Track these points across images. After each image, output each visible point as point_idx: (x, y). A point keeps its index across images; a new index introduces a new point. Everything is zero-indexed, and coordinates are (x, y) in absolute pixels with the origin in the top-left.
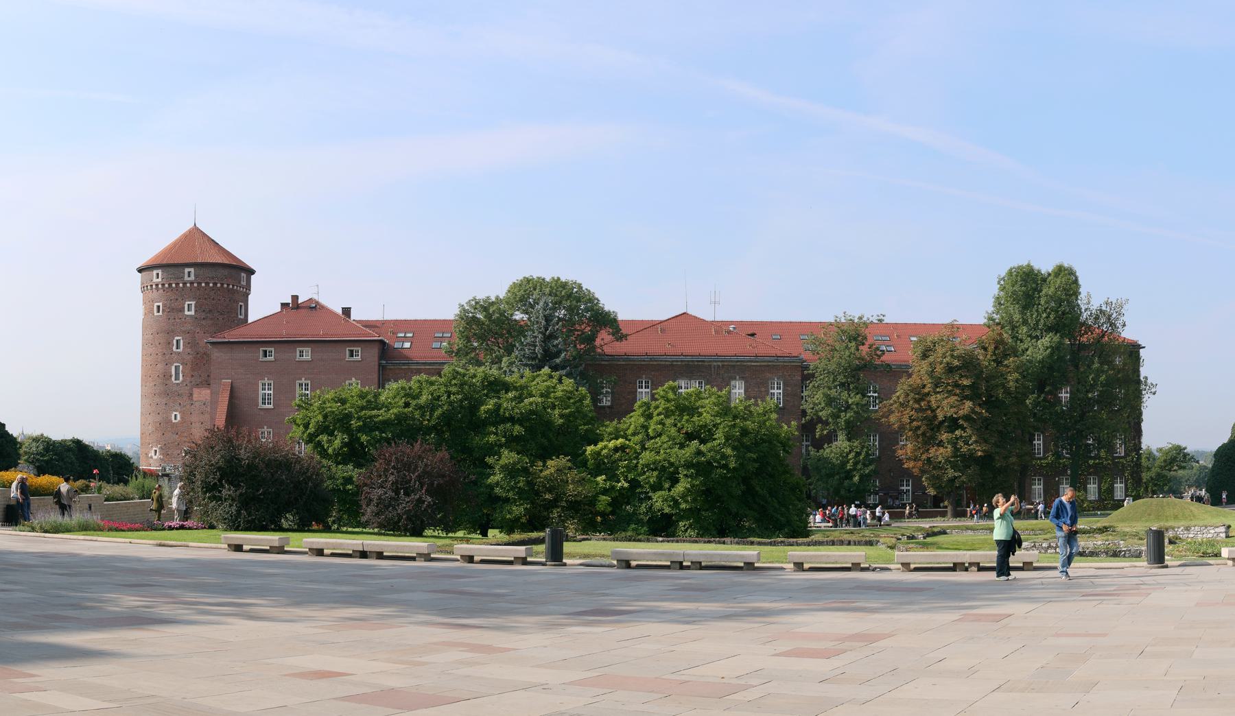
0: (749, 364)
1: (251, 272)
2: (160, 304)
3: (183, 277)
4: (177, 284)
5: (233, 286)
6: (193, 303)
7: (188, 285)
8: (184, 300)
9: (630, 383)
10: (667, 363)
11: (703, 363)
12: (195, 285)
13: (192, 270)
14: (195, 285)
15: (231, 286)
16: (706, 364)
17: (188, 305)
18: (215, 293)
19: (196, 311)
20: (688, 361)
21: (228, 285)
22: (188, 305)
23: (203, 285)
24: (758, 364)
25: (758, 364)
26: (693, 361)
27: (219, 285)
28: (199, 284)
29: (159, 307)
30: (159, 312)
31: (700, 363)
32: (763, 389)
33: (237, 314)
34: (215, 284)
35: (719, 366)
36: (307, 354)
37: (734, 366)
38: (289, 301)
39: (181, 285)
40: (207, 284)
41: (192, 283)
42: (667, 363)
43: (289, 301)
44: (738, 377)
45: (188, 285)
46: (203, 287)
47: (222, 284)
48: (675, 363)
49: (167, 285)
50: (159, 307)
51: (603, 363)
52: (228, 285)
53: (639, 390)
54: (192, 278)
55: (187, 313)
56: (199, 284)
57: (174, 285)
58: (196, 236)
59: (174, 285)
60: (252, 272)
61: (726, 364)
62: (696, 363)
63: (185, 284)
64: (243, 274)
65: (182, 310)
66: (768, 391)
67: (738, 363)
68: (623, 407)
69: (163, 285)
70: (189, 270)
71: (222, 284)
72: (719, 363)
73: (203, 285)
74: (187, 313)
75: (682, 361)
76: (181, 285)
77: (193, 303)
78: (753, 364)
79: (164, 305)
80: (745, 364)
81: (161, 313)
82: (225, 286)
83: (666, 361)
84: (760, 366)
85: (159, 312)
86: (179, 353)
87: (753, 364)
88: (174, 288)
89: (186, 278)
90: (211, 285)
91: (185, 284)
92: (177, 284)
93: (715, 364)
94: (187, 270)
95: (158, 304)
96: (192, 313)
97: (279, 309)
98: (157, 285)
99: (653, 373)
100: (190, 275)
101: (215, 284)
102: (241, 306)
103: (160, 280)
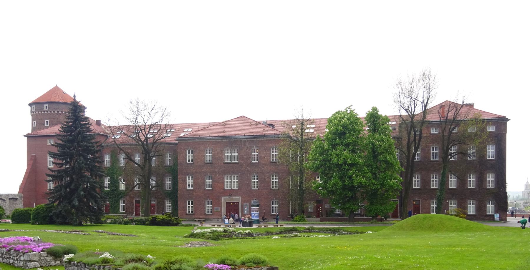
0: (261, 139)
2: (35, 121)
3: (44, 109)
4: (41, 112)
6: (48, 121)
7: (46, 112)
8: (45, 119)
9: (202, 151)
10: (220, 140)
11: (238, 140)
12: (49, 112)
13: (47, 105)
19: (49, 124)
23: (52, 112)
24: (265, 139)
25: (265, 139)
27: (60, 112)
28: (51, 111)
29: (35, 122)
31: (236, 140)
32: (268, 152)
34: (58, 112)
35: (245, 141)
37: (253, 141)
39: (43, 112)
40: (54, 111)
41: (47, 111)
42: (220, 140)
44: (255, 147)
45: (46, 112)
46: (53, 113)
47: (62, 112)
48: (223, 140)
49: (37, 113)
56: (51, 111)
57: (40, 113)
59: (40, 113)
61: (249, 139)
62: (234, 140)
65: (44, 124)
66: (259, 154)
67: (255, 139)
68: (199, 163)
69: (36, 112)
71: (62, 112)
72: (246, 140)
73: (52, 112)
75: (227, 139)
76: (43, 112)
77: (48, 121)
78: (263, 139)
80: (259, 139)
81: (35, 126)
84: (266, 140)
87: (263, 139)
88: (40, 114)
89: (45, 109)
90: (56, 112)
91: (44, 112)
92: (41, 112)
93: (244, 140)
94: (45, 105)
98: (33, 112)
99: (213, 146)
100: (46, 107)
101: (58, 112)
103: (34, 110)
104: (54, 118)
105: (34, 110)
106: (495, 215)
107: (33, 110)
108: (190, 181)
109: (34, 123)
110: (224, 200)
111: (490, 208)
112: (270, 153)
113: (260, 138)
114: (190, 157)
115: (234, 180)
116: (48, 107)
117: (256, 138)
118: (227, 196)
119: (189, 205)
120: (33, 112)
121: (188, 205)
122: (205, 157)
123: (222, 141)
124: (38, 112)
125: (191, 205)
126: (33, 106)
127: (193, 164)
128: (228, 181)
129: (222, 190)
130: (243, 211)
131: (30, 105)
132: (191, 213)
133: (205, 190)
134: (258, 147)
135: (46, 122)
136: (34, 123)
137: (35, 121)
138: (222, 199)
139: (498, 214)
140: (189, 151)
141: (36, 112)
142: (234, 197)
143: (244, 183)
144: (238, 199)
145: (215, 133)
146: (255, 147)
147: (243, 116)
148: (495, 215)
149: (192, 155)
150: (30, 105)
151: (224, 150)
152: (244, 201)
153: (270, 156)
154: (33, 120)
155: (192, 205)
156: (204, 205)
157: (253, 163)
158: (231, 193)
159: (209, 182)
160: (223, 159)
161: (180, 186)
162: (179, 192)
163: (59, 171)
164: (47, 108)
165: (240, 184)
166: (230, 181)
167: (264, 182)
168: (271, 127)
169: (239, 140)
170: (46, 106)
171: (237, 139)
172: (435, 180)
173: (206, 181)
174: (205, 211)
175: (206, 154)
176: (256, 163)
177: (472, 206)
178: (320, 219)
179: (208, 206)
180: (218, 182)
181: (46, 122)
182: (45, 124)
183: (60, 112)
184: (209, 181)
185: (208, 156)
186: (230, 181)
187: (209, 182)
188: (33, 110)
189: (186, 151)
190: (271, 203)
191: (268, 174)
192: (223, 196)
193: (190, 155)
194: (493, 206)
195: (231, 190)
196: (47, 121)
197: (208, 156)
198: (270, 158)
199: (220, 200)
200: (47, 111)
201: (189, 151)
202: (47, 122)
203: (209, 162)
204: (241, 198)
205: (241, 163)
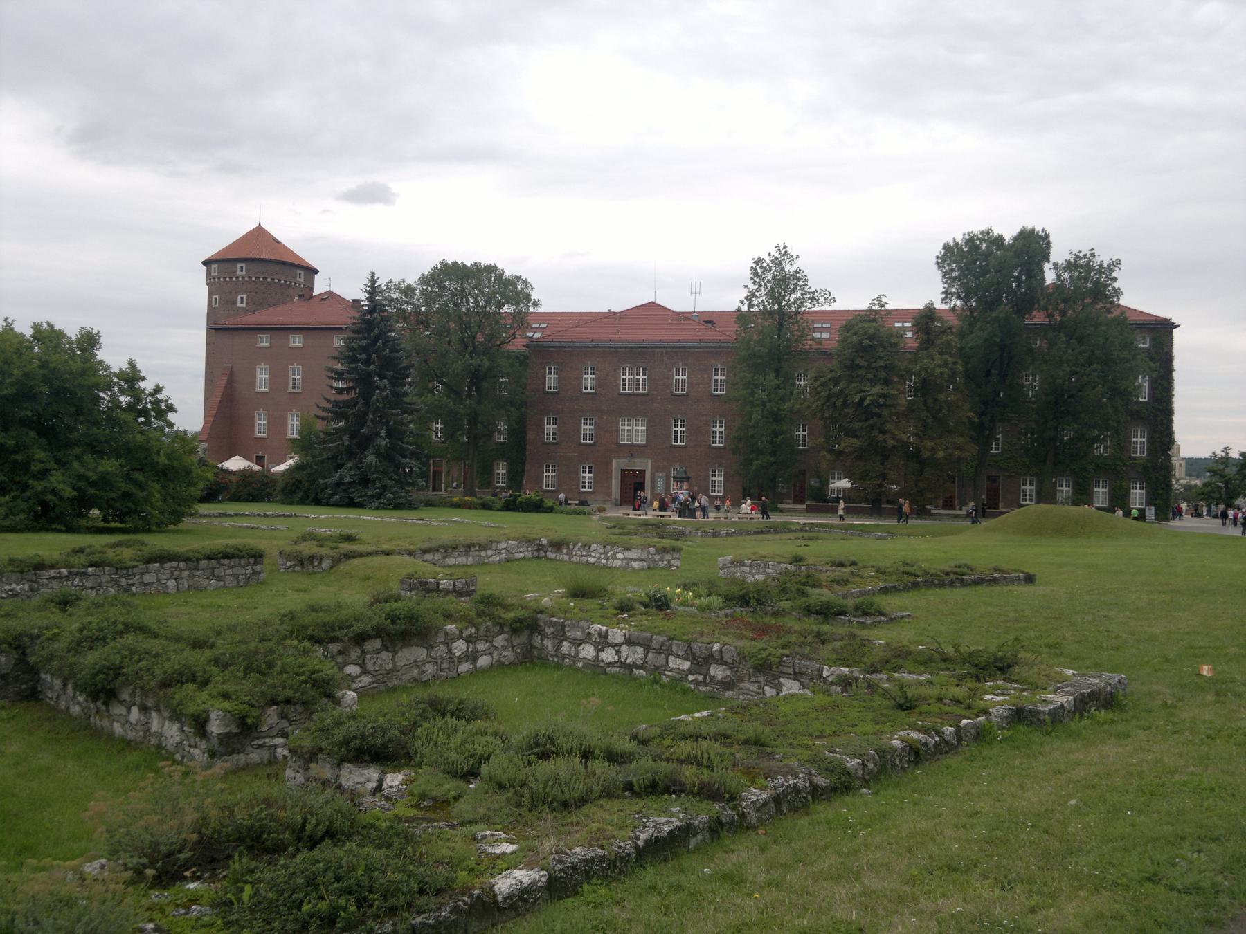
0: (692, 350)
1: (316, 272)
2: (217, 297)
3: (236, 272)
4: (231, 278)
5: (285, 281)
6: (245, 296)
7: (240, 279)
12: (246, 279)
13: (243, 265)
14: (246, 279)
15: (283, 282)
16: (650, 350)
18: (266, 287)
19: (247, 304)
20: (631, 348)
21: (279, 280)
23: (254, 279)
26: (636, 348)
27: (269, 280)
28: (250, 278)
29: (216, 299)
32: (706, 376)
35: (662, 352)
36: (296, 341)
39: (234, 279)
40: (257, 278)
41: (243, 277)
44: (680, 364)
45: (240, 279)
47: (273, 279)
50: (216, 299)
51: (551, 349)
52: (279, 280)
53: (585, 376)
54: (244, 273)
55: (239, 305)
56: (250, 278)
57: (228, 279)
58: (259, 232)
59: (228, 279)
60: (316, 272)
63: (237, 278)
64: (299, 271)
65: (235, 302)
69: (219, 278)
71: (273, 279)
72: (664, 350)
73: (254, 279)
74: (239, 305)
75: (626, 348)
76: (234, 279)
77: (245, 296)
79: (220, 298)
81: (217, 306)
82: (276, 281)
83: (610, 348)
89: (239, 273)
90: (261, 279)
91: (237, 278)
92: (231, 278)
94: (239, 265)
95: (215, 297)
98: (214, 279)
100: (241, 270)
101: (265, 279)
103: (216, 274)
104: (256, 290)
105: (216, 274)
106: (1147, 508)
107: (213, 274)
108: (550, 428)
109: (213, 300)
110: (617, 465)
111: (1138, 496)
112: (711, 378)
113: (691, 348)
114: (551, 379)
115: (637, 428)
117: (684, 347)
118: (624, 457)
119: (547, 474)
120: (214, 279)
121: (545, 474)
122: (581, 381)
123: (617, 352)
124: (225, 278)
125: (551, 474)
126: (213, 266)
127: (557, 393)
128: (626, 428)
129: (613, 446)
130: (653, 488)
131: (206, 263)
132: (550, 488)
133: (581, 444)
134: (686, 364)
135: (239, 299)
136: (213, 300)
137: (217, 297)
138: (614, 462)
139: (1153, 508)
140: (550, 368)
141: (219, 278)
142: (637, 461)
143: (657, 432)
144: (644, 464)
145: (602, 334)
146: (680, 364)
147: (652, 302)
148: (1147, 508)
149: (556, 376)
150: (206, 263)
151: (619, 369)
152: (656, 469)
153: (709, 383)
154: (210, 294)
155: (554, 474)
156: (578, 474)
157: (676, 395)
158: (633, 451)
159: (588, 428)
160: (618, 385)
161: (530, 435)
162: (528, 447)
163: (336, 402)
164: (242, 271)
165: (650, 434)
166: (630, 428)
167: (697, 431)
168: (710, 325)
169: (650, 350)
170: (242, 268)
171: (646, 348)
172: (1139, 440)
173: (583, 427)
174: (578, 485)
175: (585, 376)
176: (683, 395)
177: (1101, 490)
178: (804, 506)
179: (584, 475)
180: (607, 430)
181: (239, 299)
182: (236, 303)
183: (269, 280)
184: (588, 427)
185: (589, 379)
186: (630, 428)
187: (588, 428)
188: (213, 274)
189: (544, 368)
190: (709, 473)
191: (705, 418)
192: (615, 457)
193: (553, 376)
194: (1144, 491)
195: (632, 445)
197: (589, 379)
198: (710, 387)
199: (609, 464)
200: (243, 277)
201: (550, 368)
202: (242, 298)
203: (589, 390)
204: (650, 462)
205: (653, 394)
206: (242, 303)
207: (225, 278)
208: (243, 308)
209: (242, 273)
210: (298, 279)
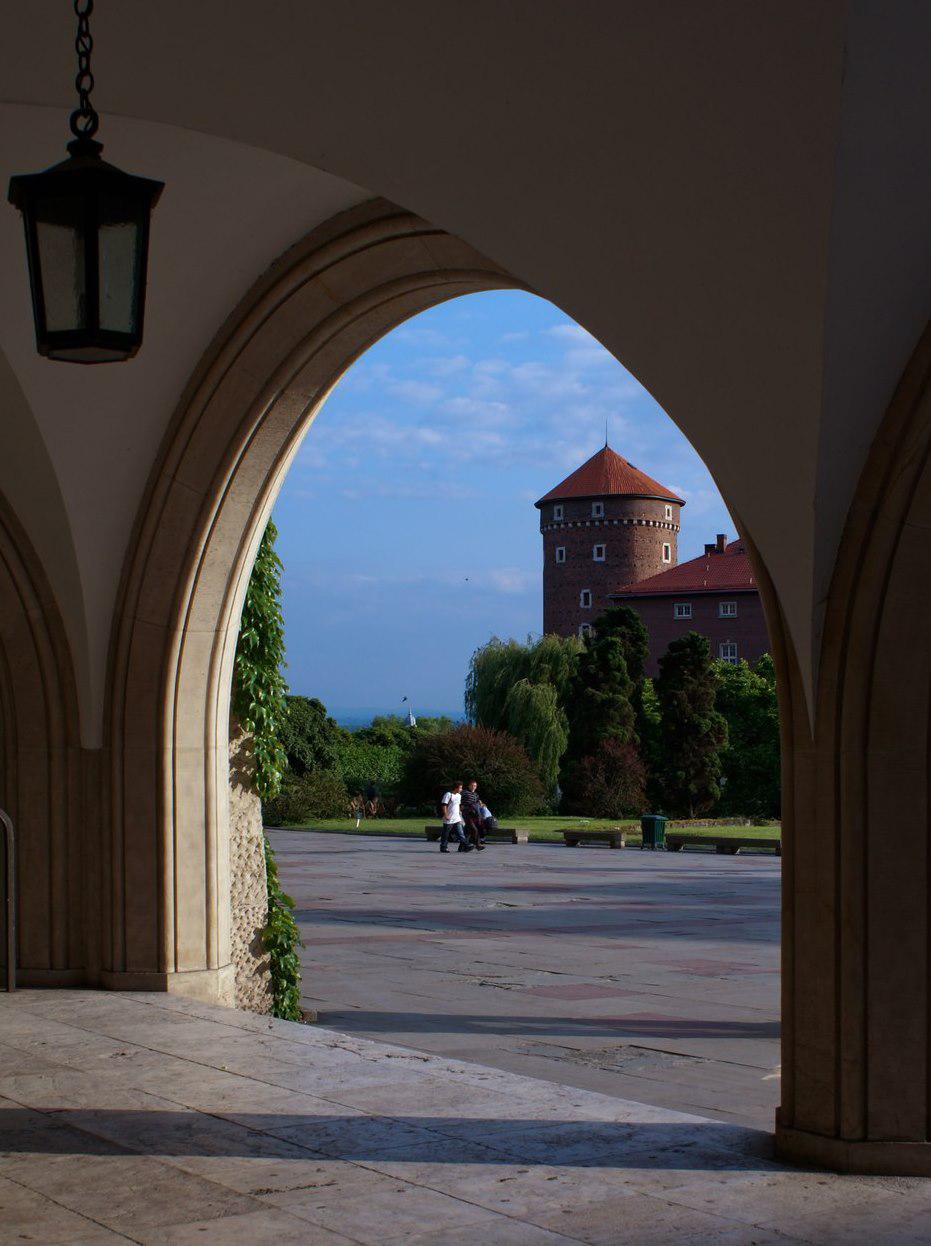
2: (563, 548)
4: (583, 523)
6: (603, 546)
7: (597, 523)
8: (592, 543)
12: (606, 523)
13: (601, 504)
14: (606, 523)
17: (598, 549)
19: (607, 556)
22: (598, 549)
23: (615, 522)
29: (561, 552)
30: (561, 558)
33: (661, 558)
38: (714, 541)
39: (588, 524)
41: (601, 521)
43: (714, 541)
45: (597, 523)
50: (561, 552)
54: (602, 514)
55: (596, 559)
56: (611, 521)
57: (579, 524)
59: (579, 524)
60: (682, 504)
63: (592, 522)
69: (566, 524)
70: (598, 504)
73: (615, 522)
74: (596, 559)
76: (588, 524)
77: (603, 546)
81: (564, 560)
85: (561, 558)
86: (588, 610)
89: (594, 515)
91: (592, 522)
92: (583, 523)
94: (594, 505)
96: (603, 559)
97: (702, 552)
98: (559, 525)
102: (667, 547)
103: (562, 518)
105: (562, 518)
107: (556, 518)
109: (557, 553)
116: (605, 509)
120: (559, 525)
124: (575, 524)
131: (538, 505)
135: (595, 551)
136: (557, 553)
137: (563, 548)
141: (566, 524)
150: (538, 505)
170: (598, 508)
181: (595, 551)
196: (599, 546)
202: (600, 550)
206: (600, 555)
207: (575, 524)
208: (601, 563)
209: (599, 516)
210: (666, 517)
